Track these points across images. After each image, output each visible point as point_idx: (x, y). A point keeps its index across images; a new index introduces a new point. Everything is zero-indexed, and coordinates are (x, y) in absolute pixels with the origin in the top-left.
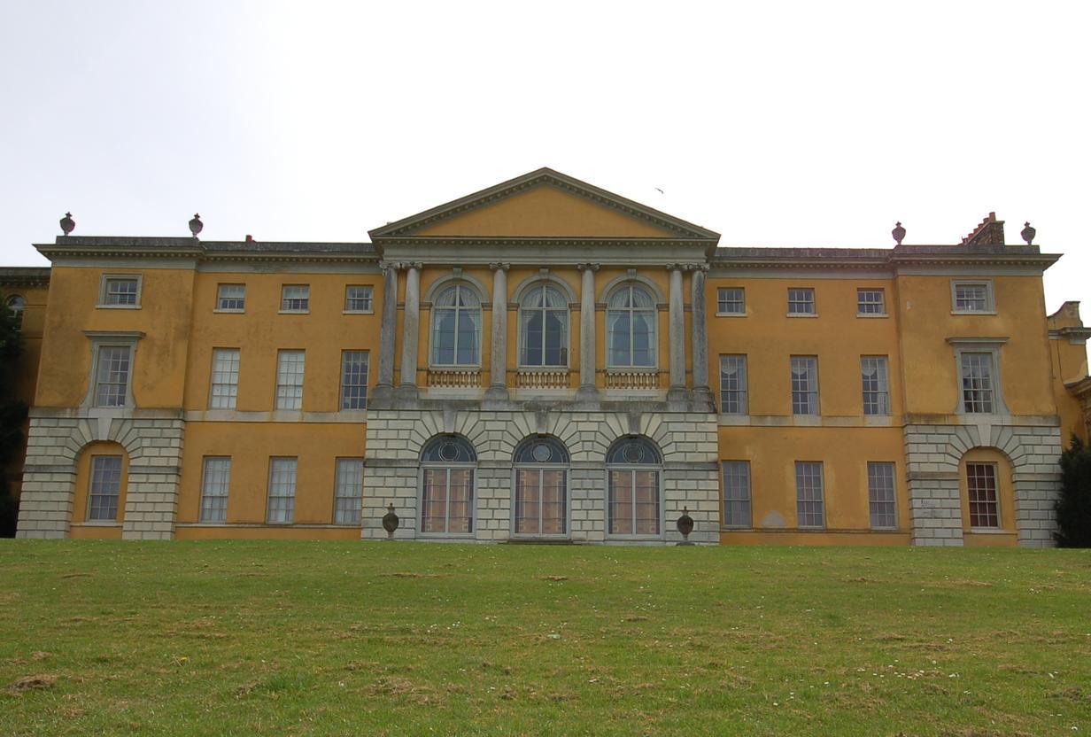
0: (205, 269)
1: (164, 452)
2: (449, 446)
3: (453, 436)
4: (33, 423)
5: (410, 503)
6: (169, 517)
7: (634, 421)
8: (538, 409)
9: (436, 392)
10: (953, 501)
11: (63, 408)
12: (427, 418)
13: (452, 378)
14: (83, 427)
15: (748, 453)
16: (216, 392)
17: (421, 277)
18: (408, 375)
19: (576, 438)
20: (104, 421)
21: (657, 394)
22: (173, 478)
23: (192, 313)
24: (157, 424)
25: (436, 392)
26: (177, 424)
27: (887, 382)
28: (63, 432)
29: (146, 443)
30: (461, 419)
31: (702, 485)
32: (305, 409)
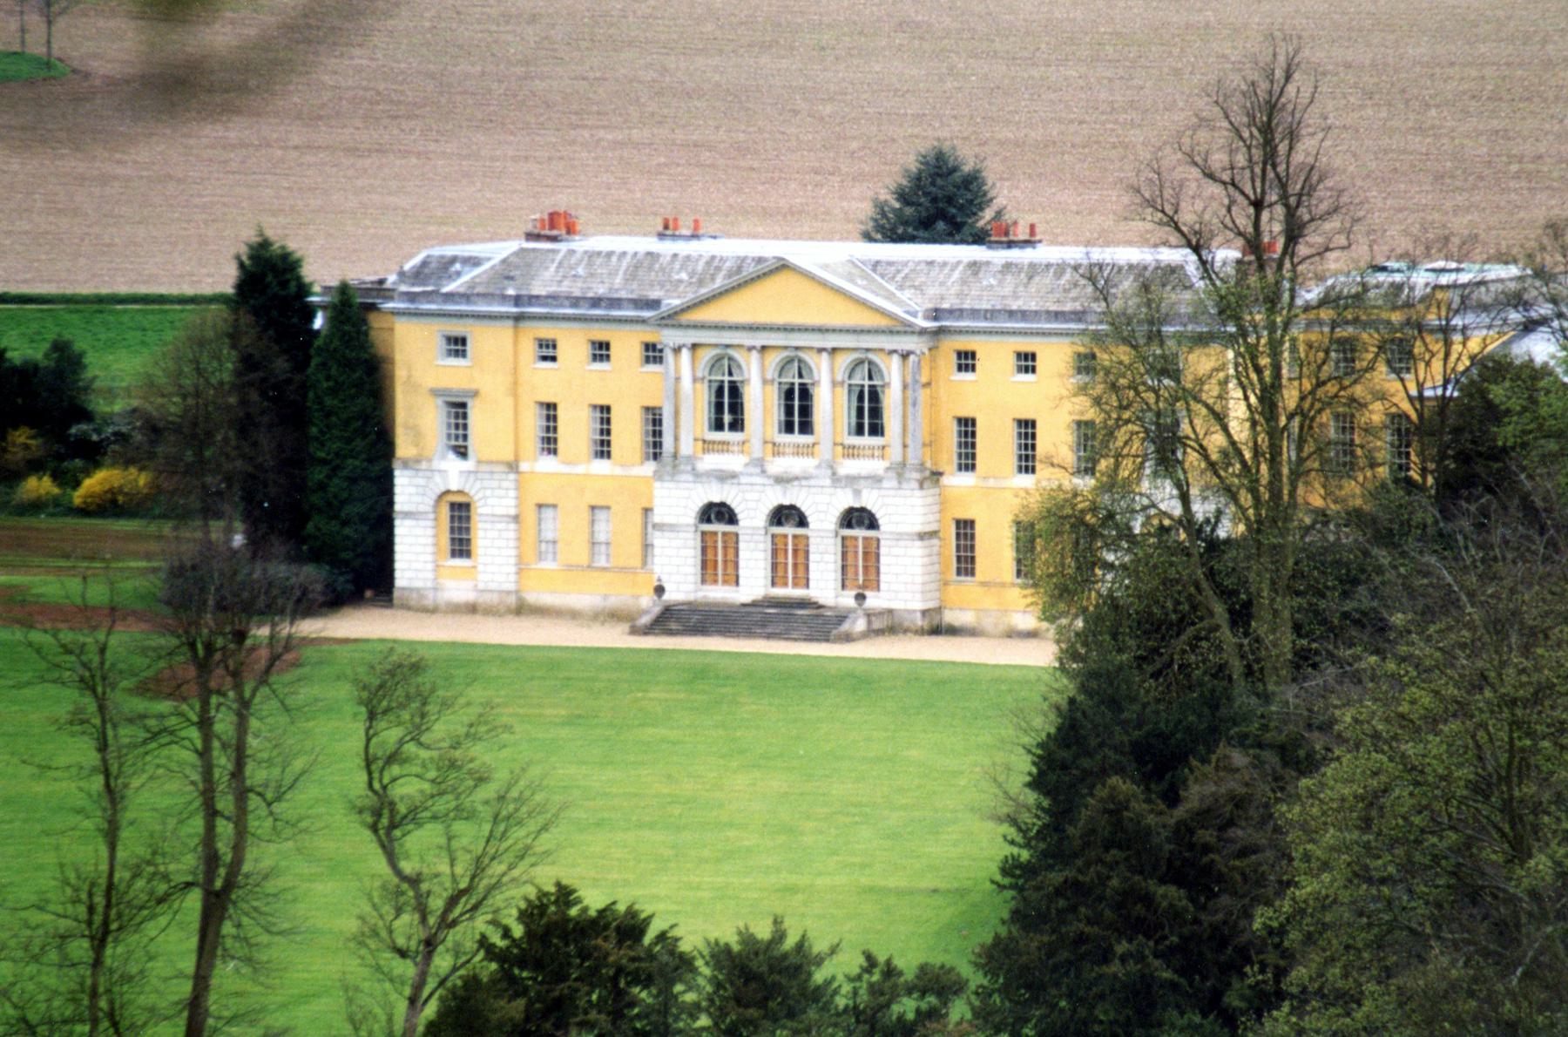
18: (686, 448)
20: (452, 473)
22: (513, 526)
24: (496, 476)
29: (488, 492)
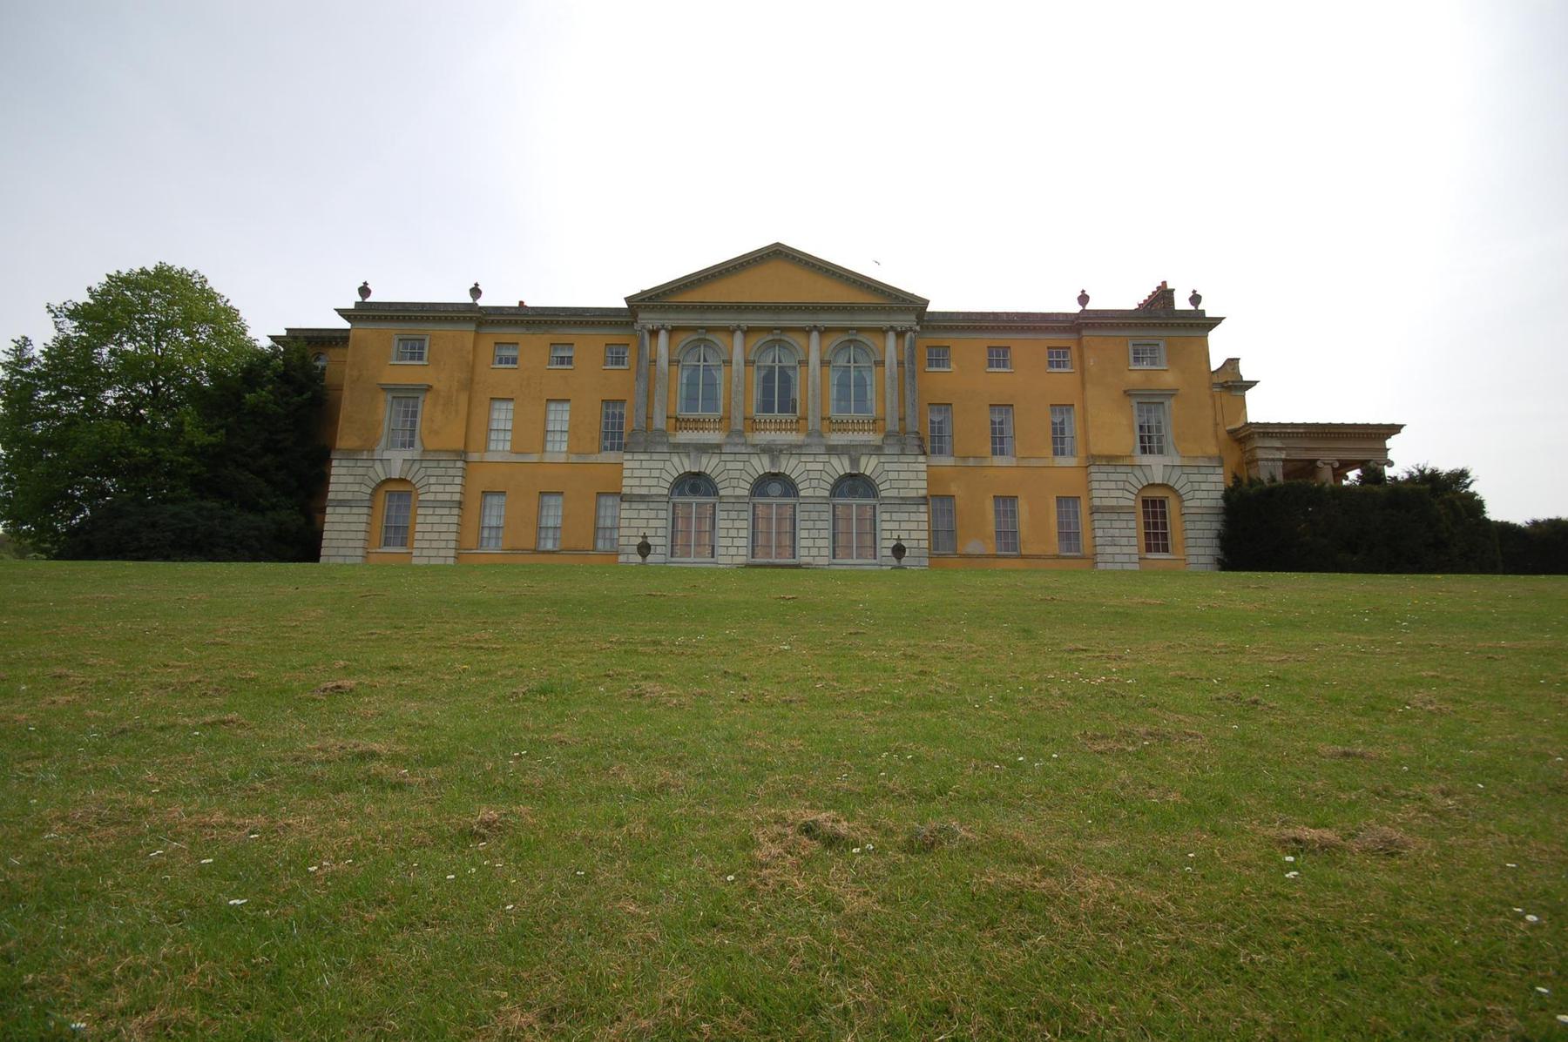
0: (485, 330)
1: (448, 488)
2: (694, 483)
3: (698, 474)
4: (334, 463)
5: (661, 532)
6: (452, 545)
7: (855, 462)
8: (772, 451)
9: (684, 437)
10: (1132, 530)
11: (361, 450)
12: (675, 459)
13: (697, 425)
14: (378, 466)
15: (953, 489)
16: (493, 436)
17: (670, 338)
18: (659, 422)
19: (804, 476)
20: (396, 462)
21: (874, 438)
22: (456, 511)
23: (472, 369)
25: (684, 437)
26: (459, 464)
27: (1073, 427)
28: (361, 471)
29: (433, 480)
30: (704, 460)
31: (914, 517)
32: (570, 451)
